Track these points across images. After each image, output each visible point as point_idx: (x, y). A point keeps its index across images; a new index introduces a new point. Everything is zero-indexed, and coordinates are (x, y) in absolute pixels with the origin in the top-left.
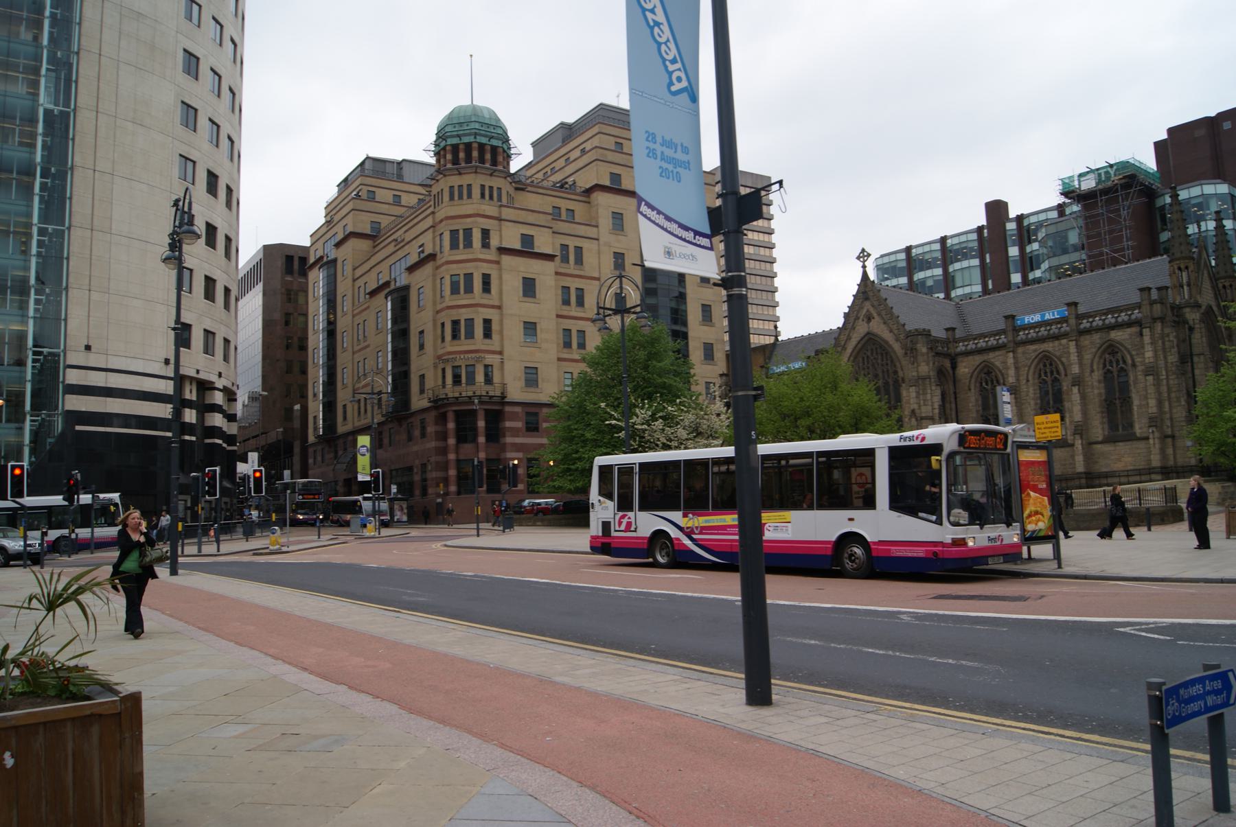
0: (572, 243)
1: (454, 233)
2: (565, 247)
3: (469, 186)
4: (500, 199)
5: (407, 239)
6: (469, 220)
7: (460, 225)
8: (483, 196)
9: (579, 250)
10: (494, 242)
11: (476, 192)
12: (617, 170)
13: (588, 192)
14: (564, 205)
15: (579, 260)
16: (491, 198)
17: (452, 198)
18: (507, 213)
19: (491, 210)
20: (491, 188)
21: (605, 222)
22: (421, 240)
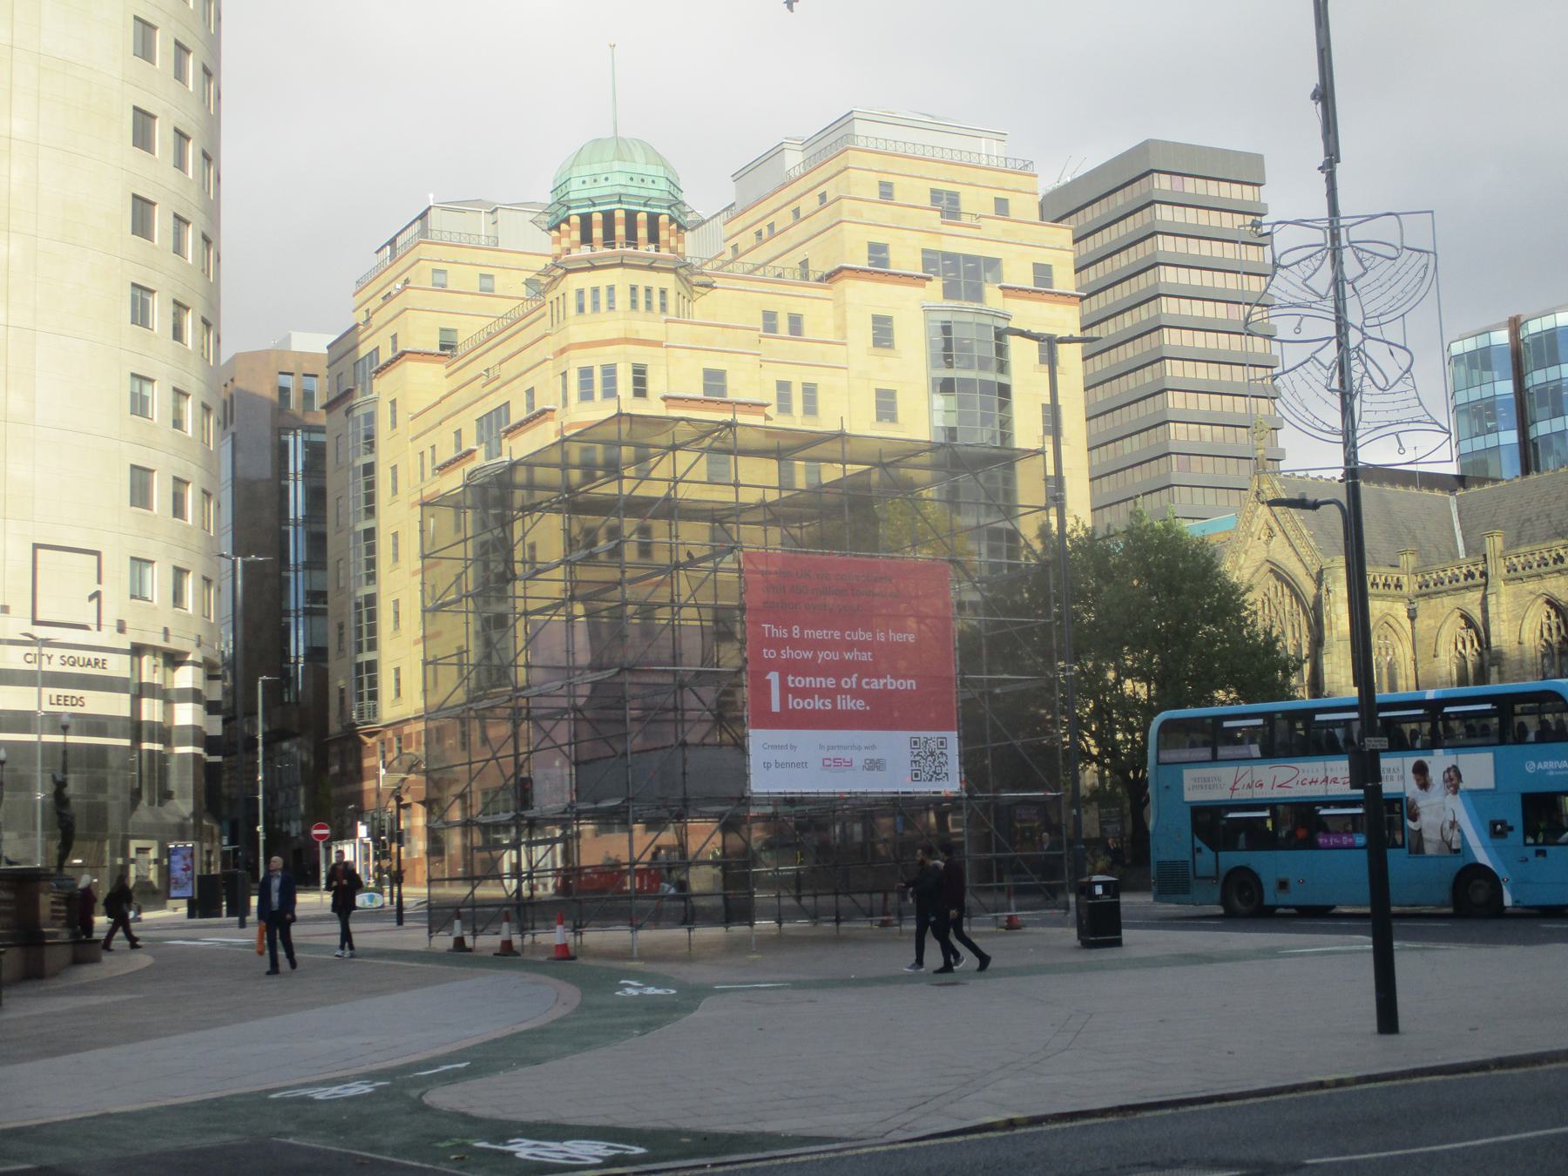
0: (797, 377)
1: (586, 373)
2: (783, 387)
3: (611, 289)
4: (663, 306)
5: (505, 377)
6: (610, 349)
7: (596, 359)
8: (634, 303)
9: (810, 391)
10: (655, 386)
11: (622, 298)
12: (879, 237)
13: (831, 277)
14: (784, 306)
15: (810, 408)
16: (649, 304)
17: (581, 309)
18: (678, 333)
19: (648, 325)
20: (648, 290)
21: (863, 333)
22: (529, 381)
